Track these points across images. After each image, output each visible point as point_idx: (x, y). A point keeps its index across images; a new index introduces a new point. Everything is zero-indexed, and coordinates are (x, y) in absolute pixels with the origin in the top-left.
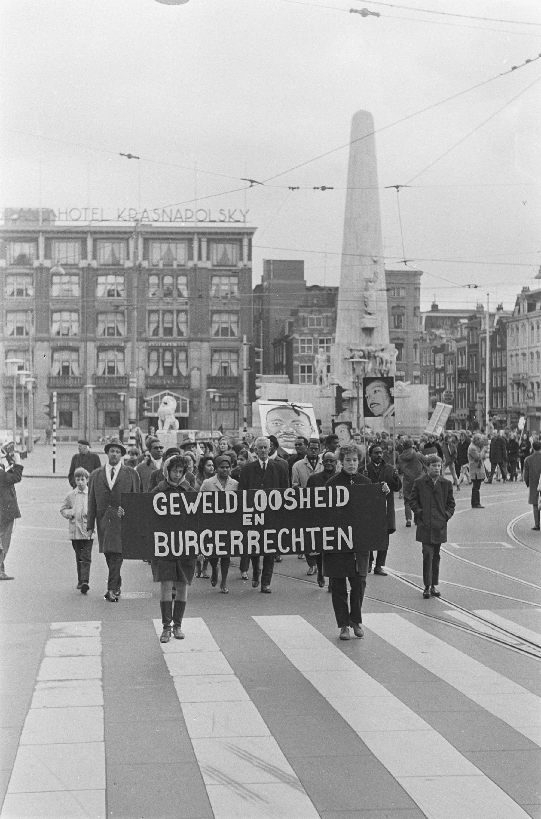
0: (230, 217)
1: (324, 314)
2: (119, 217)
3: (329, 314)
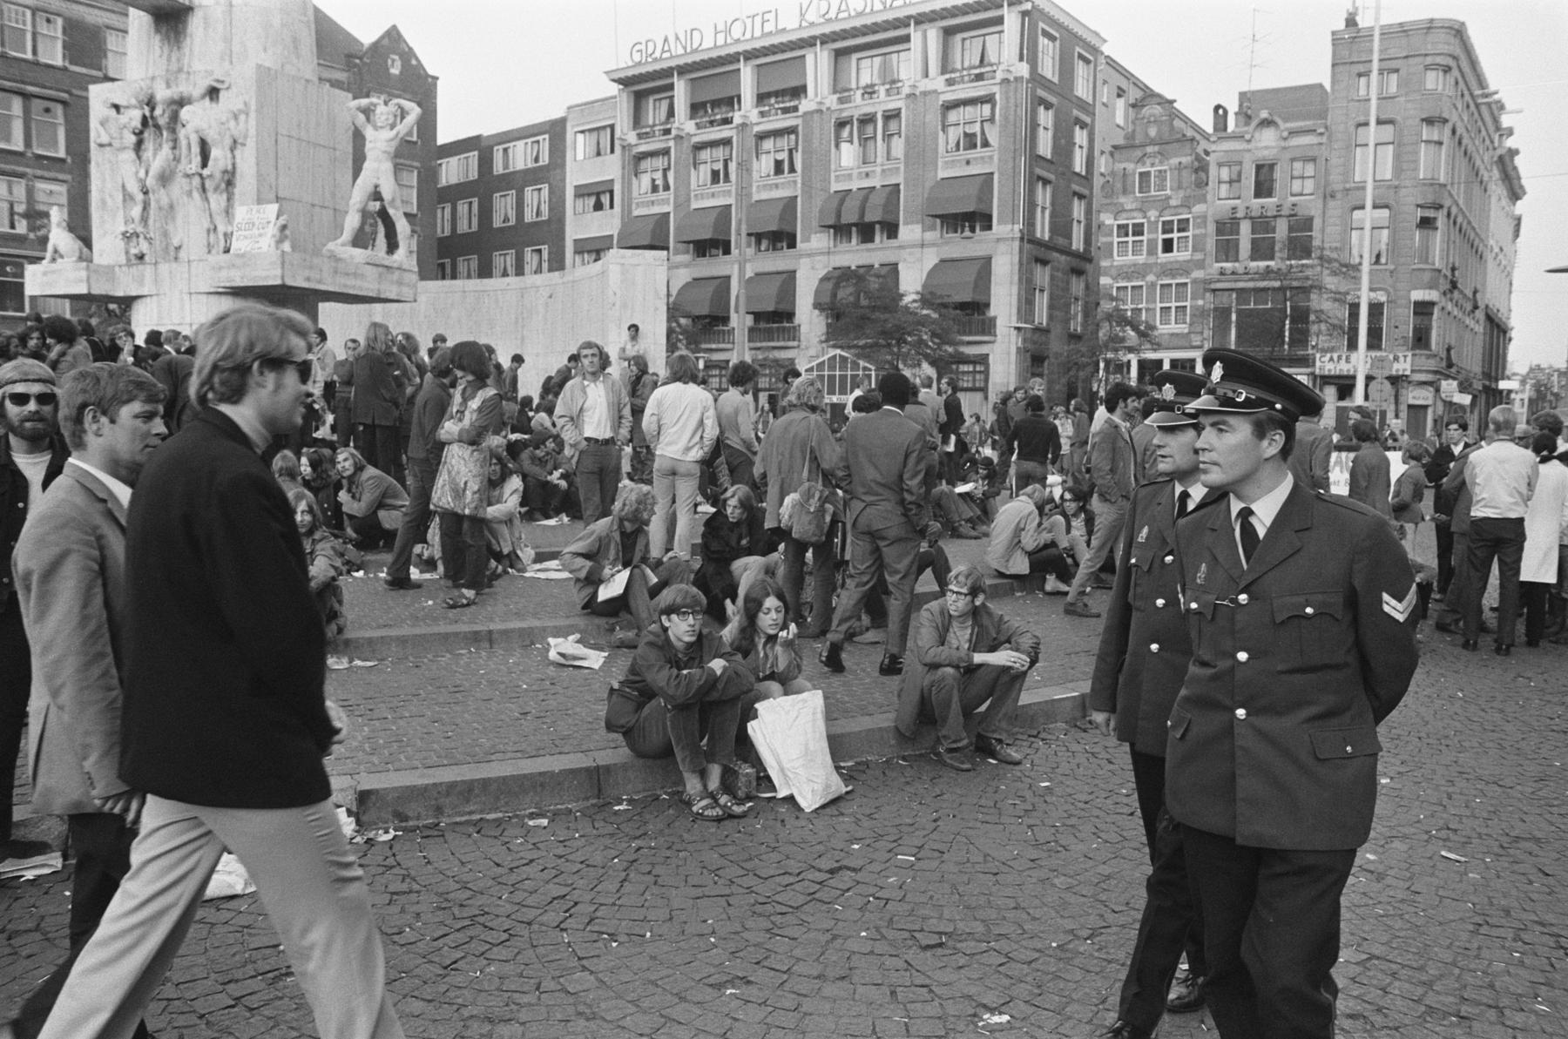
1: (1174, 161)
3: (1186, 160)
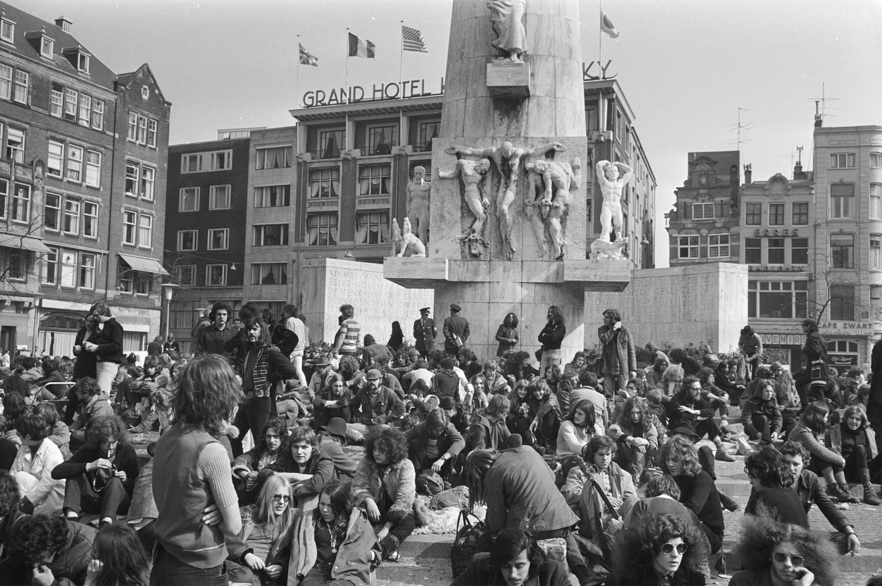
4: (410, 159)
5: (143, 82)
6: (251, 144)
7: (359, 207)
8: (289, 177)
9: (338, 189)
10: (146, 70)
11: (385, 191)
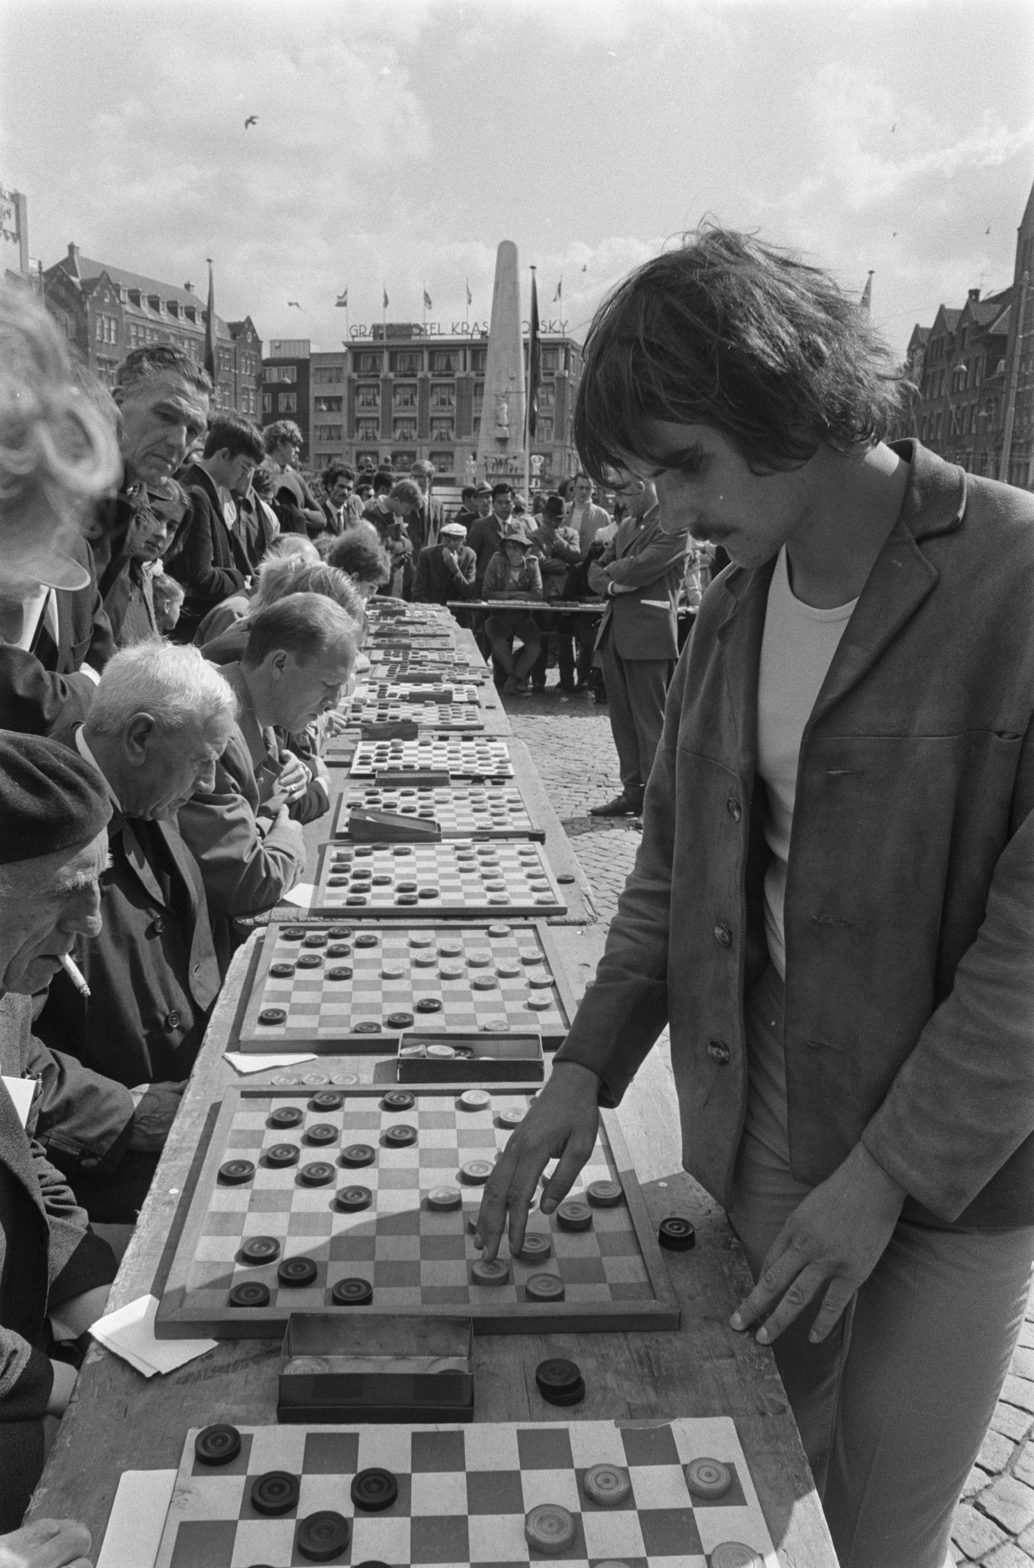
0: (551, 328)
2: (453, 330)
4: (431, 382)
5: (248, 330)
6: (311, 364)
7: (395, 415)
8: (341, 390)
9: (379, 400)
10: (249, 320)
11: (412, 403)
